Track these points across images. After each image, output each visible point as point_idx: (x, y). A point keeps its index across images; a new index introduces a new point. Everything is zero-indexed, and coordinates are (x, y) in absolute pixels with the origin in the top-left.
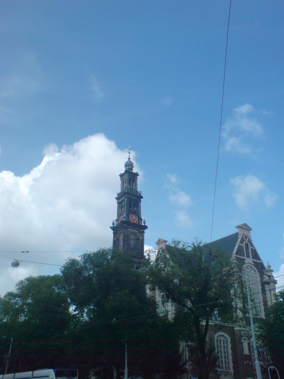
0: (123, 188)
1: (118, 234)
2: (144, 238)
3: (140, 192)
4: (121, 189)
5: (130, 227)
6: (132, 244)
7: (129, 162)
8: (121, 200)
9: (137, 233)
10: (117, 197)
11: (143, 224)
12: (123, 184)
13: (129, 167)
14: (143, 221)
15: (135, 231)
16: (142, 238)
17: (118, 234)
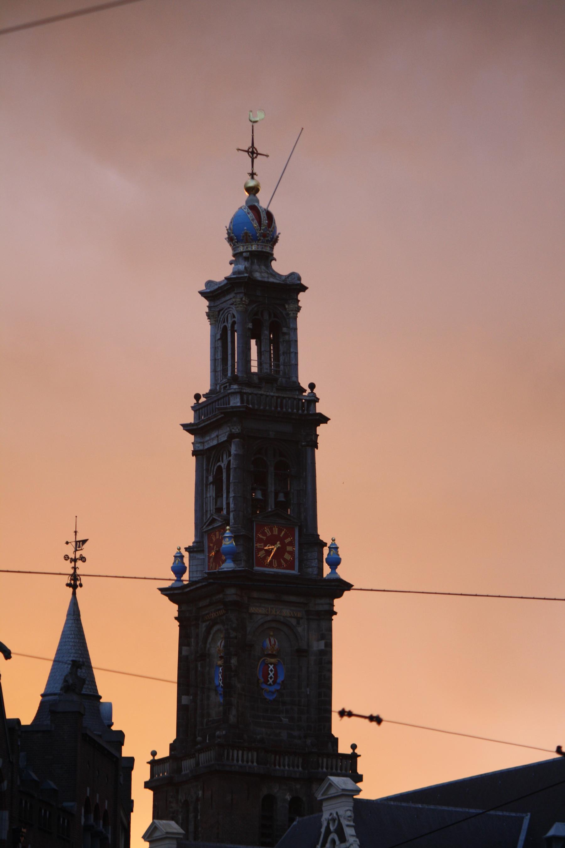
0: (225, 371)
1: (203, 626)
2: (329, 645)
4: (214, 371)
5: (255, 595)
6: (271, 681)
7: (251, 216)
8: (212, 440)
9: (294, 622)
10: (192, 421)
11: (327, 570)
12: (219, 344)
13: (254, 248)
14: (326, 551)
15: (286, 612)
16: (322, 645)
17: (203, 626)
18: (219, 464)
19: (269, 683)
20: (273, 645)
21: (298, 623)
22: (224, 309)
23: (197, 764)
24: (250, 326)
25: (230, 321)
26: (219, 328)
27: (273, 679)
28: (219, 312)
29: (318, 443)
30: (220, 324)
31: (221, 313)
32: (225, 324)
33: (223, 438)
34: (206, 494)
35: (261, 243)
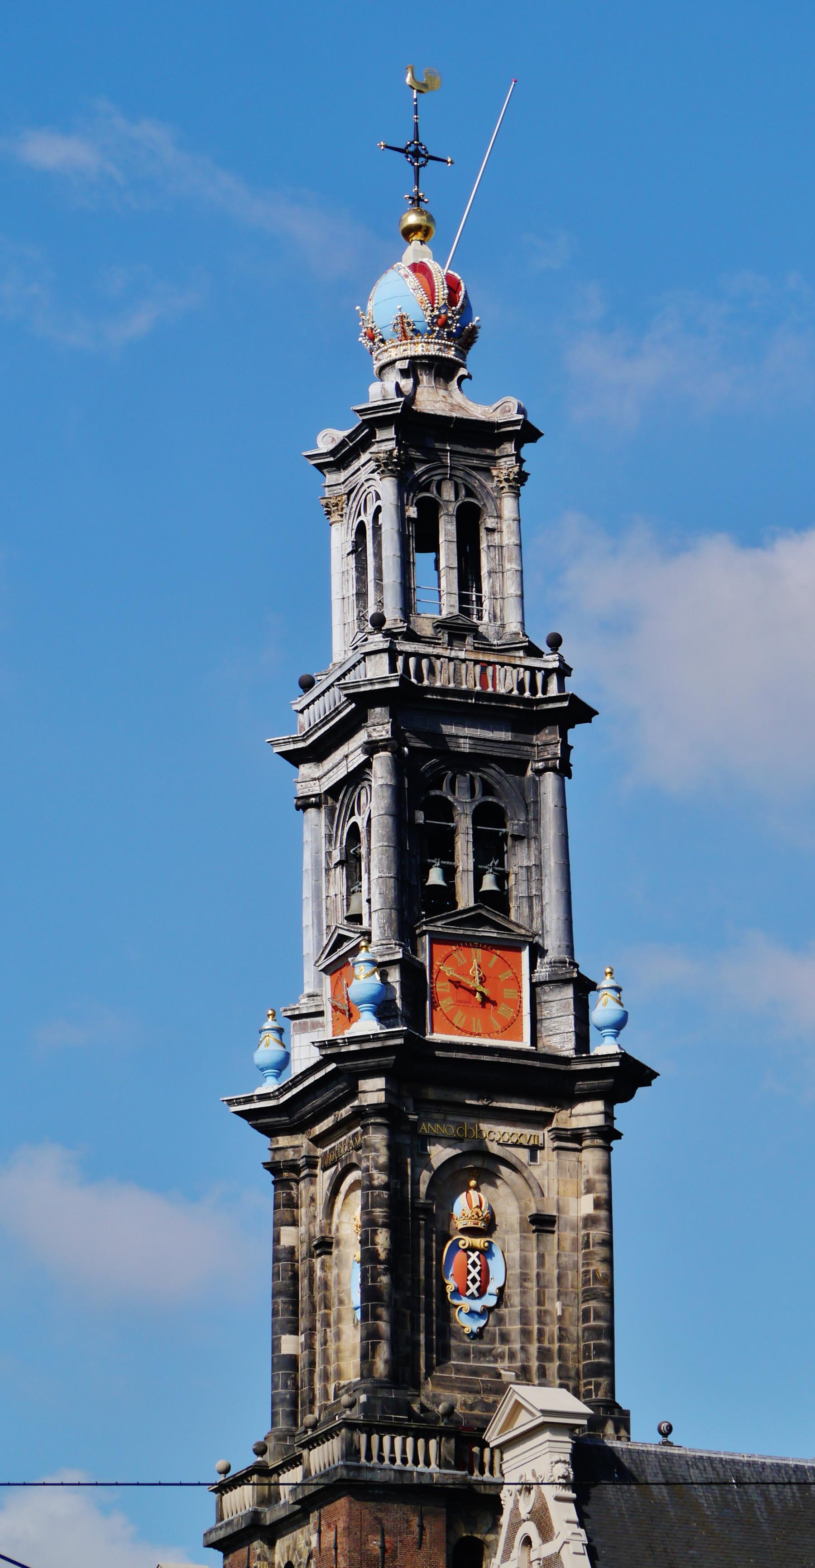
3: (555, 642)
17: (324, 1178)
18: (353, 820)
19: (468, 1293)
20: (477, 1207)
21: (533, 1158)
22: (358, 486)
23: (307, 1473)
24: (412, 512)
25: (371, 510)
26: (350, 530)
27: (478, 1284)
28: (349, 494)
29: (572, 765)
30: (351, 520)
31: (353, 495)
32: (360, 519)
33: (359, 758)
34: (328, 889)
35: (435, 338)
